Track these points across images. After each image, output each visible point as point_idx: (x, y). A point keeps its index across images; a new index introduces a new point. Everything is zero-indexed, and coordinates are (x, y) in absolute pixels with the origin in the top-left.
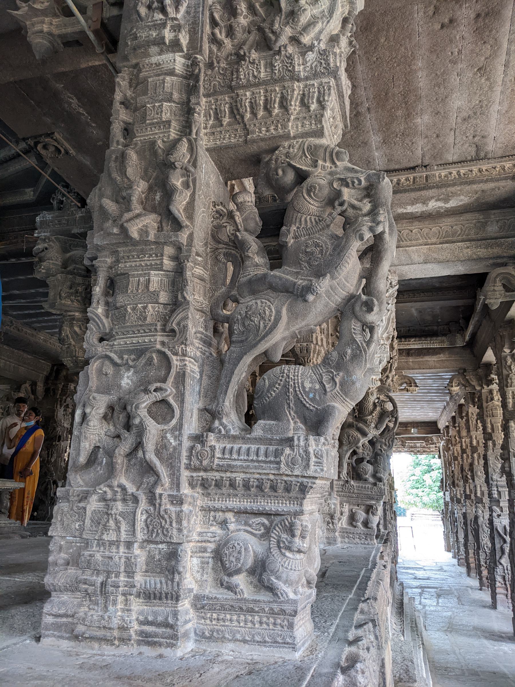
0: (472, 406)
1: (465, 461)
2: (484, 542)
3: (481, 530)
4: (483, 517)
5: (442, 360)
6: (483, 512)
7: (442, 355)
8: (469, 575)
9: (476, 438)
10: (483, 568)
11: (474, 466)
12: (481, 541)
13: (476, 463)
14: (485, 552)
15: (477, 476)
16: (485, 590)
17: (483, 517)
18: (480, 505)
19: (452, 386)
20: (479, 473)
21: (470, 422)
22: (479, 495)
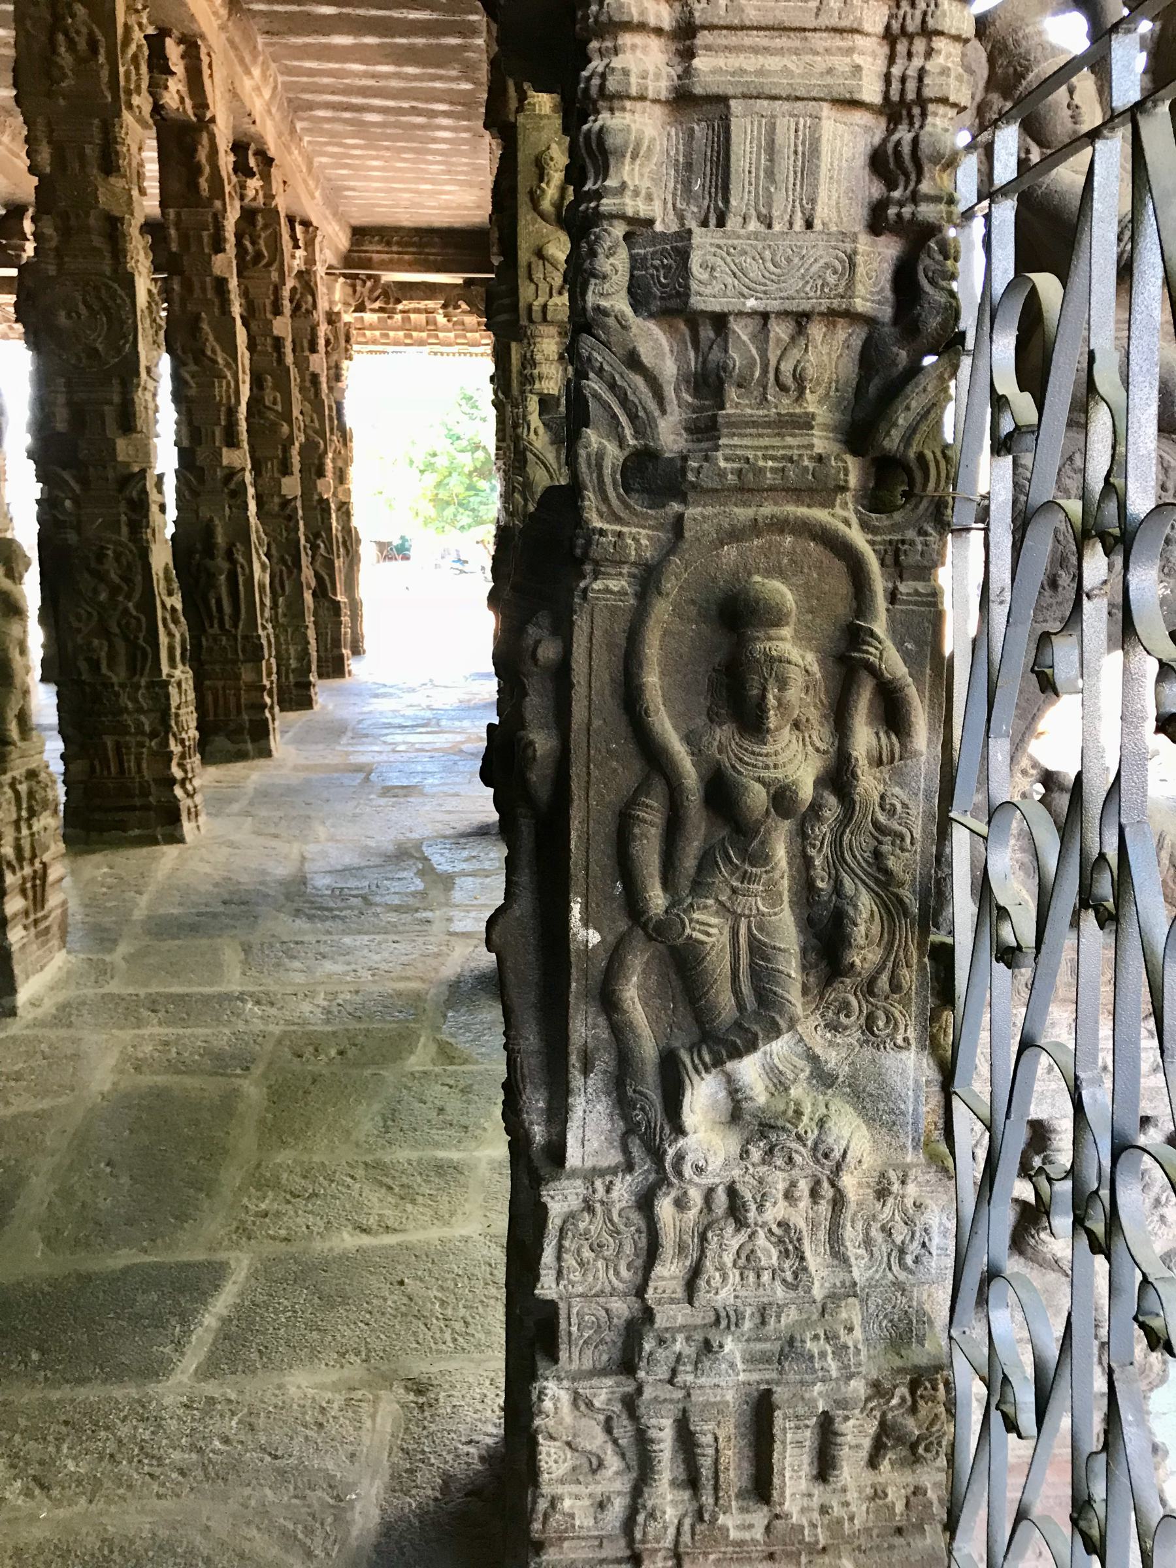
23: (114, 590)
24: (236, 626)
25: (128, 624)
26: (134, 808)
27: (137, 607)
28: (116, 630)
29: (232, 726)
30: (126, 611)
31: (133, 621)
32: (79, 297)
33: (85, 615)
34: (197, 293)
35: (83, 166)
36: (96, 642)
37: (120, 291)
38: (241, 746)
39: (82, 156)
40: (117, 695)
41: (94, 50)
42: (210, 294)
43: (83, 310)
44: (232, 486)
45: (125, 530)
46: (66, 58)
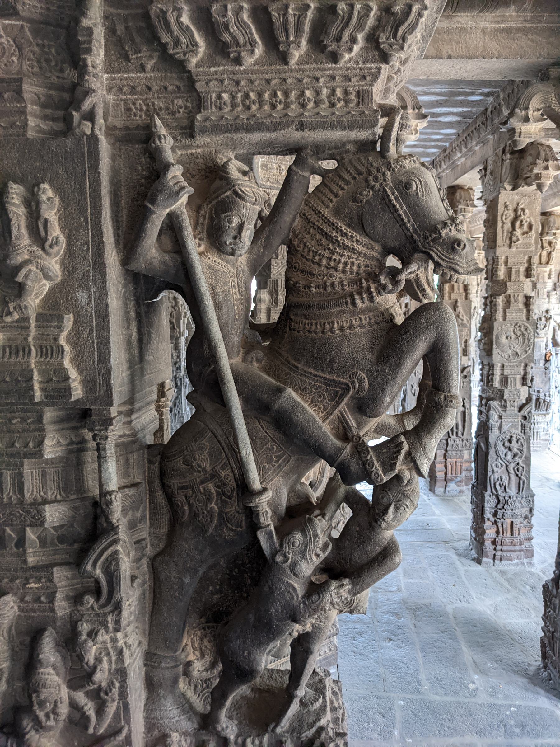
0: (509, 187)
1: (446, 297)
2: (496, 476)
3: (492, 452)
4: (500, 428)
5: (508, 30)
6: (500, 417)
7: (511, 11)
8: (432, 489)
9: (506, 263)
10: (488, 524)
11: (496, 325)
12: (490, 473)
13: (499, 316)
14: (497, 496)
15: (498, 344)
16: (487, 563)
17: (500, 428)
18: (495, 404)
19: (526, 120)
20: (503, 340)
21: (500, 224)
22: (497, 384)
23: (515, 455)
24: (463, 435)
25: (518, 470)
26: (514, 551)
27: (523, 461)
28: (512, 471)
29: (459, 479)
30: (518, 464)
31: (521, 468)
32: (512, 329)
33: (500, 466)
34: (456, 290)
35: (518, 276)
36: (504, 478)
37: (530, 328)
38: (461, 488)
39: (518, 271)
40: (514, 501)
41: (530, 227)
42: (462, 290)
43: (513, 336)
44: (465, 373)
45: (520, 428)
46: (518, 232)
